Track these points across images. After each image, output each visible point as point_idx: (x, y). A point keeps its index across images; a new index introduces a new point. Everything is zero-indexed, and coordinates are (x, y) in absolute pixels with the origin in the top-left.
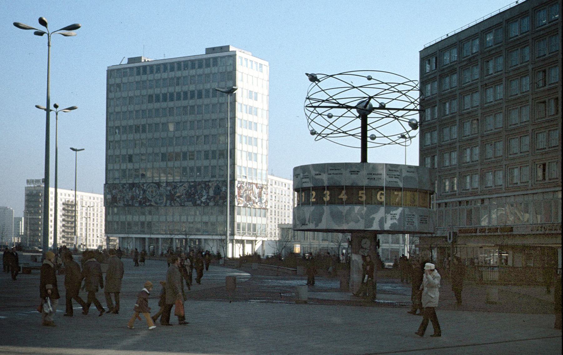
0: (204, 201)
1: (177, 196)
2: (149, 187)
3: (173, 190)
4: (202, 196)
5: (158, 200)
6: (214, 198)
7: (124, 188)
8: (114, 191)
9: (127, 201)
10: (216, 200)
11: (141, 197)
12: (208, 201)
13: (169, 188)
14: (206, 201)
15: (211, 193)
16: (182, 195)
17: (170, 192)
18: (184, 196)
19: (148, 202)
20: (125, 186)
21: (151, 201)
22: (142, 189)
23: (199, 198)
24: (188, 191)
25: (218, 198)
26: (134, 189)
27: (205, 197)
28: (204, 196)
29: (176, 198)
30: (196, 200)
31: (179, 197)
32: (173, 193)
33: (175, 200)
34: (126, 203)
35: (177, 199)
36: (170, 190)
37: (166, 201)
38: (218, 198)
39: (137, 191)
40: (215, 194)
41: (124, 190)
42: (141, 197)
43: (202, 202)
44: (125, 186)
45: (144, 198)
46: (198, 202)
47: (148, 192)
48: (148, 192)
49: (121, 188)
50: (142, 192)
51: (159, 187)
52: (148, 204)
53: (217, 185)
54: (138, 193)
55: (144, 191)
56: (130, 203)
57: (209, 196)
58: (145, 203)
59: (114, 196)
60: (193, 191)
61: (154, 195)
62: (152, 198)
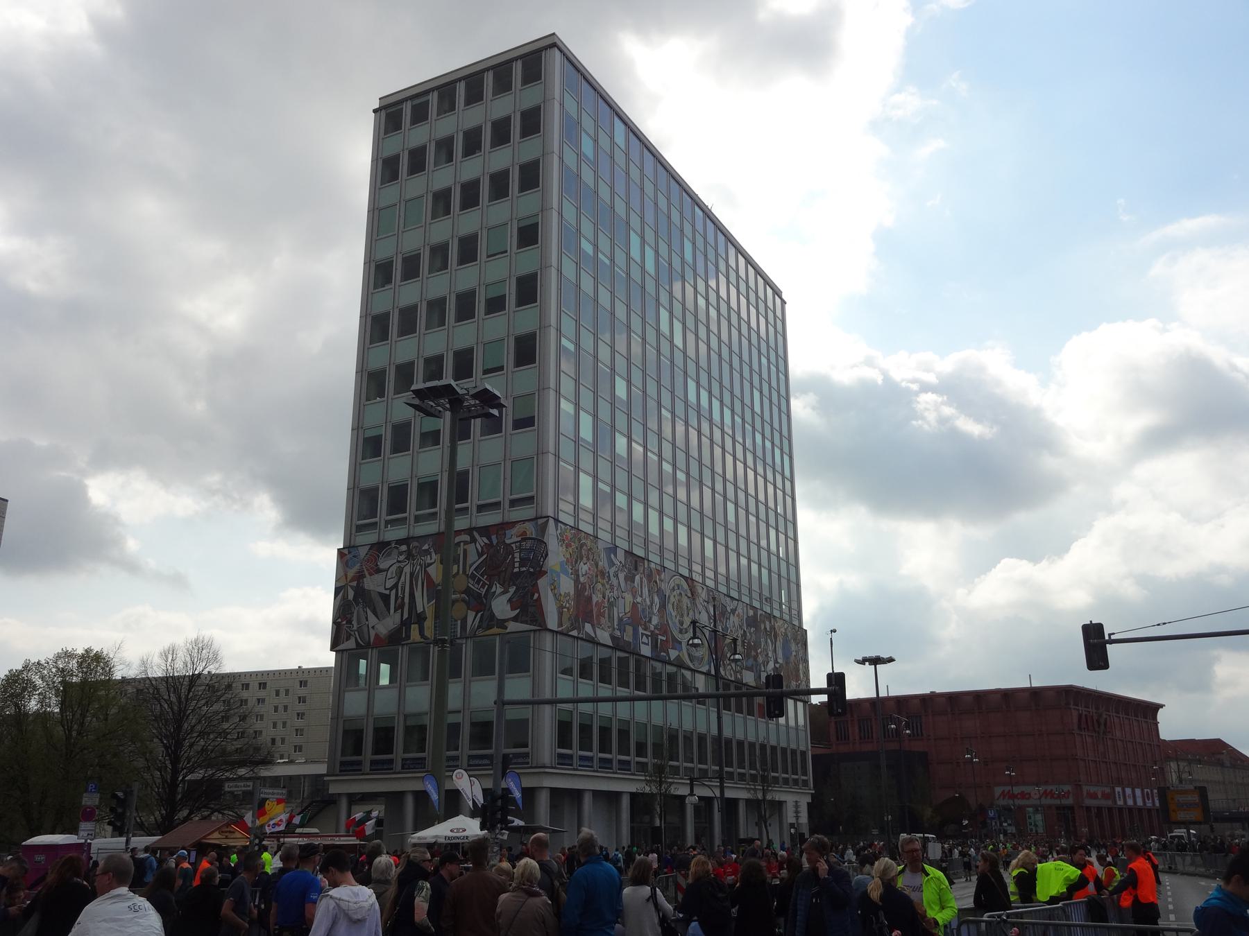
2: (673, 589)
3: (720, 621)
11: (655, 620)
23: (763, 663)
26: (637, 578)
34: (618, 633)
39: (646, 591)
42: (655, 620)
49: (603, 563)
50: (656, 599)
52: (673, 654)
54: (648, 603)
58: (665, 647)
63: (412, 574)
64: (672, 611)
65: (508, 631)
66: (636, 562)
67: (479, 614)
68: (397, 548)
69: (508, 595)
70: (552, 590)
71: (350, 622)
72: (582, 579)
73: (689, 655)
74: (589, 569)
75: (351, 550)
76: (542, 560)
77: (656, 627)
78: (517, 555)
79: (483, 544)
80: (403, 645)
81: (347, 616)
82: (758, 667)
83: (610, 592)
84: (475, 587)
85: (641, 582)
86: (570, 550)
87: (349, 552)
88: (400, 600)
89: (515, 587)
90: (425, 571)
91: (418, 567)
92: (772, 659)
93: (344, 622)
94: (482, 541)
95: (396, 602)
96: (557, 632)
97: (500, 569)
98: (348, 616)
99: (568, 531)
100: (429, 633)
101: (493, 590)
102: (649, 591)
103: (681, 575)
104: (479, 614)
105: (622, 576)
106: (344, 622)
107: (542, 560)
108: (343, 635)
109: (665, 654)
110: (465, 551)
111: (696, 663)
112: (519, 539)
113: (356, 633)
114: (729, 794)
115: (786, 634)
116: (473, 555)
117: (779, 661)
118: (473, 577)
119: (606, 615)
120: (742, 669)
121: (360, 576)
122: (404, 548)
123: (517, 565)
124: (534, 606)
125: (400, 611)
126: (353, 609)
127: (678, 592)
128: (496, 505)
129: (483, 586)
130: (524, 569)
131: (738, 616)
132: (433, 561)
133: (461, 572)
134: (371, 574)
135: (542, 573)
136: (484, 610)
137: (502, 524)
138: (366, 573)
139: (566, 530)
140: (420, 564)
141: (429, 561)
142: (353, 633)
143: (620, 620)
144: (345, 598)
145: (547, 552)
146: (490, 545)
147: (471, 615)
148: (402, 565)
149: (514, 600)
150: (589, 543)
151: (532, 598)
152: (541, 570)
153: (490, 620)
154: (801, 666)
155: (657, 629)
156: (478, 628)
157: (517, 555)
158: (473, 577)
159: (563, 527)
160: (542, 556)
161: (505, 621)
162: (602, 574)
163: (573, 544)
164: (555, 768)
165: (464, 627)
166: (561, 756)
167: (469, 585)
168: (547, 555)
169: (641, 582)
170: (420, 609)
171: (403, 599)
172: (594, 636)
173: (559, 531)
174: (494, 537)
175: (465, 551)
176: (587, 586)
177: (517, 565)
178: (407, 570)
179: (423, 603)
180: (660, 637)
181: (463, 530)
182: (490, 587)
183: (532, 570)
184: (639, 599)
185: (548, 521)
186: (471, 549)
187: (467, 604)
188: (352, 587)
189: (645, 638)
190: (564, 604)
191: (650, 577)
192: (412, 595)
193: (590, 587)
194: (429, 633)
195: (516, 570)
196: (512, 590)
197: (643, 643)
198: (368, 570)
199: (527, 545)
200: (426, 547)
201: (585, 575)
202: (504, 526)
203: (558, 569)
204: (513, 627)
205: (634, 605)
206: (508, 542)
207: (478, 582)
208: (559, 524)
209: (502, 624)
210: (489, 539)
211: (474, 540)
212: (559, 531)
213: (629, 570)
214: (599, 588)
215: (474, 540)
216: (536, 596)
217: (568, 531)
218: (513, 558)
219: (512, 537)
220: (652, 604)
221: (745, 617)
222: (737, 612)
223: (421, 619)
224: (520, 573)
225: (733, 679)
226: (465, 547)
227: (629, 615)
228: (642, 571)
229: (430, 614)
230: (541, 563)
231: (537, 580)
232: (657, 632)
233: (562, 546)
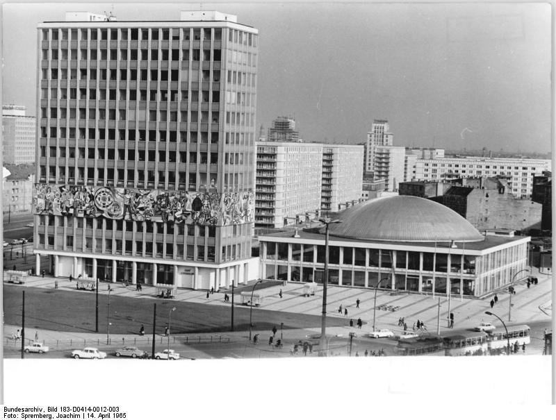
0: (178, 217)
1: (139, 208)
4: (177, 210)
5: (112, 210)
6: (193, 214)
7: (62, 191)
8: (48, 195)
9: (67, 209)
11: (87, 205)
12: (184, 217)
13: (128, 196)
14: (181, 218)
15: (189, 208)
17: (130, 202)
18: (150, 208)
20: (63, 189)
21: (102, 212)
22: (90, 196)
23: (172, 213)
24: (155, 203)
27: (181, 212)
28: (179, 210)
29: (138, 210)
31: (142, 209)
33: (138, 212)
34: (65, 211)
35: (141, 212)
36: (130, 199)
38: (198, 214)
39: (82, 196)
40: (193, 208)
41: (62, 194)
43: (175, 218)
46: (171, 218)
47: (97, 199)
48: (97, 199)
50: (88, 198)
51: (114, 194)
52: (98, 215)
54: (83, 200)
55: (92, 198)
56: (71, 211)
60: (164, 203)
61: (107, 204)
62: (104, 207)
119: (60, 206)
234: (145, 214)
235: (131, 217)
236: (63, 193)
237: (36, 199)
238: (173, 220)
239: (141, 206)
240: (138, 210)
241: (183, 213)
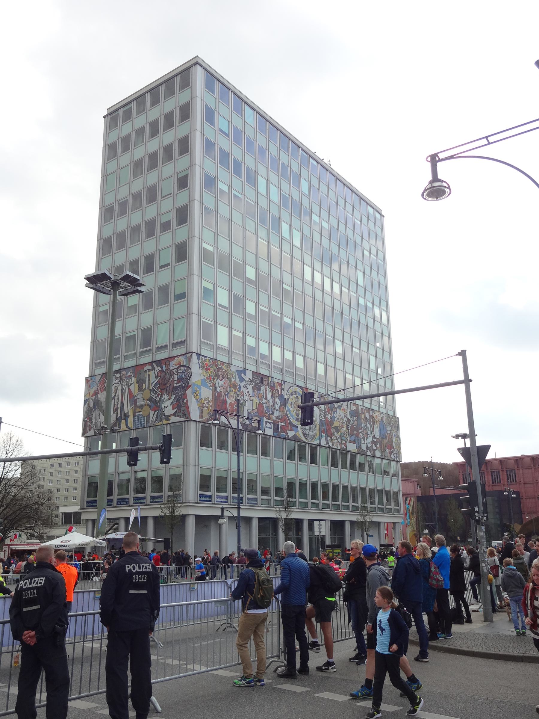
1: (334, 428)
2: (292, 394)
3: (329, 413)
7: (242, 380)
8: (219, 383)
10: (382, 445)
11: (277, 413)
12: (374, 447)
14: (372, 446)
16: (342, 427)
17: (325, 416)
18: (344, 429)
19: (291, 430)
20: (243, 375)
25: (384, 446)
26: (263, 388)
27: (370, 439)
30: (361, 443)
31: (337, 429)
32: (329, 417)
33: (332, 435)
36: (325, 410)
37: (320, 434)
39: (269, 396)
41: (242, 384)
42: (277, 413)
44: (243, 375)
45: (284, 418)
49: (236, 380)
50: (278, 401)
52: (291, 434)
53: (382, 421)
54: (271, 403)
57: (374, 437)
58: (284, 429)
59: (220, 394)
60: (356, 423)
63: (122, 391)
64: (290, 408)
65: (170, 422)
66: (262, 378)
67: (156, 413)
68: (115, 375)
69: (171, 401)
70: (194, 396)
71: (91, 420)
72: (218, 390)
73: (304, 434)
74: (224, 383)
75: (92, 378)
76: (189, 379)
77: (277, 418)
78: (176, 376)
79: (158, 371)
80: (118, 432)
81: (90, 416)
82: (359, 441)
83: (241, 397)
84: (154, 397)
85: (266, 391)
86: (209, 372)
87: (91, 379)
88: (116, 406)
89: (174, 396)
90: (129, 388)
91: (125, 386)
92: (371, 436)
93: (88, 420)
94: (158, 368)
95: (114, 408)
96: (199, 422)
97: (167, 385)
98: (91, 416)
99: (208, 361)
100: (130, 425)
101: (163, 398)
102: (272, 396)
103: (298, 386)
104: (156, 413)
105: (250, 387)
106: (88, 420)
107: (189, 379)
108: (88, 428)
109: (284, 434)
110: (149, 375)
111: (309, 439)
112: (177, 367)
113: (94, 426)
114: (294, 516)
115: (382, 421)
116: (152, 377)
117: (376, 436)
118: (153, 390)
120: (346, 442)
121: (96, 393)
122: (118, 375)
123: (175, 382)
124: (184, 406)
125: (116, 412)
126: (93, 412)
127: (295, 396)
128: (166, 347)
129: (158, 396)
130: (179, 384)
131: (344, 410)
132: (133, 382)
133: (147, 388)
134: (102, 392)
135: (188, 387)
136: (158, 410)
137: (169, 358)
138: (99, 391)
139: (206, 360)
140: (126, 385)
141: (131, 382)
142: (92, 426)
143: (249, 413)
144: (89, 406)
145: (191, 374)
146: (162, 371)
147: (152, 413)
148: (117, 385)
149: (174, 403)
150: (224, 367)
151: (183, 402)
152: (188, 384)
153: (161, 416)
154: (394, 440)
155: (278, 418)
156: (155, 421)
157: (176, 376)
158: (153, 390)
159: (203, 358)
160: (189, 376)
161: (169, 416)
162: (235, 386)
163: (211, 368)
164: (198, 503)
165: (148, 421)
166: (201, 496)
167: (151, 395)
168: (191, 375)
169: (266, 391)
170: (126, 411)
171: (117, 405)
172: (227, 423)
173: (200, 361)
174: (164, 366)
175: (149, 375)
176: (223, 394)
177: (175, 382)
178: (120, 388)
179: (128, 408)
180: (280, 424)
181: (147, 363)
182: (162, 396)
183: (183, 385)
184: (264, 401)
185: (192, 355)
186: (152, 373)
187: (150, 406)
188: (92, 400)
189: (268, 425)
190: (204, 405)
191: (273, 388)
192: (122, 403)
193: (225, 394)
194: (130, 425)
195: (175, 385)
196: (173, 397)
197: (266, 427)
198: (100, 389)
199: (181, 370)
200: (129, 374)
201: (221, 387)
202: (170, 359)
203: (200, 384)
204: (173, 419)
205: (260, 405)
206: (171, 369)
207: (155, 394)
208: (201, 357)
209: (167, 418)
210: (162, 368)
211: (153, 369)
212: (200, 361)
213: (257, 384)
214: (232, 395)
215: (153, 369)
216: (185, 400)
217: (208, 361)
218: (174, 378)
219: (173, 365)
220: (274, 404)
221: (349, 410)
222: (342, 408)
223: (126, 416)
224: (178, 387)
225: (339, 448)
226: (149, 373)
227: (256, 410)
228: (266, 384)
229: (131, 414)
230: (188, 380)
231: (186, 390)
232: (278, 420)
233: (202, 370)
234: (341, 437)
235: (327, 442)
236: (244, 383)
237: (200, 388)
238: (365, 450)
239: (336, 424)
240: (333, 430)
241: (373, 442)
